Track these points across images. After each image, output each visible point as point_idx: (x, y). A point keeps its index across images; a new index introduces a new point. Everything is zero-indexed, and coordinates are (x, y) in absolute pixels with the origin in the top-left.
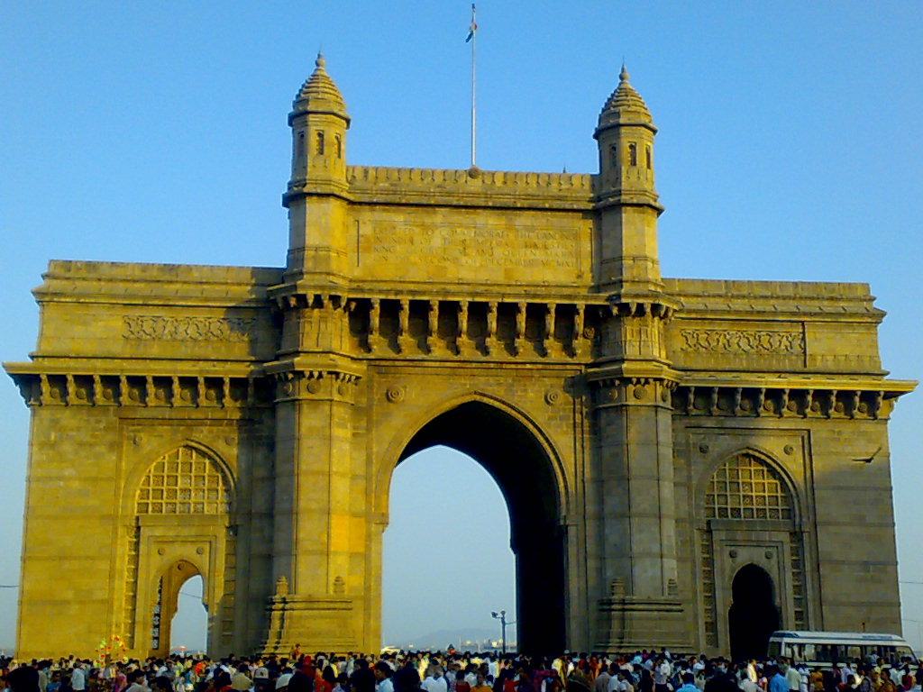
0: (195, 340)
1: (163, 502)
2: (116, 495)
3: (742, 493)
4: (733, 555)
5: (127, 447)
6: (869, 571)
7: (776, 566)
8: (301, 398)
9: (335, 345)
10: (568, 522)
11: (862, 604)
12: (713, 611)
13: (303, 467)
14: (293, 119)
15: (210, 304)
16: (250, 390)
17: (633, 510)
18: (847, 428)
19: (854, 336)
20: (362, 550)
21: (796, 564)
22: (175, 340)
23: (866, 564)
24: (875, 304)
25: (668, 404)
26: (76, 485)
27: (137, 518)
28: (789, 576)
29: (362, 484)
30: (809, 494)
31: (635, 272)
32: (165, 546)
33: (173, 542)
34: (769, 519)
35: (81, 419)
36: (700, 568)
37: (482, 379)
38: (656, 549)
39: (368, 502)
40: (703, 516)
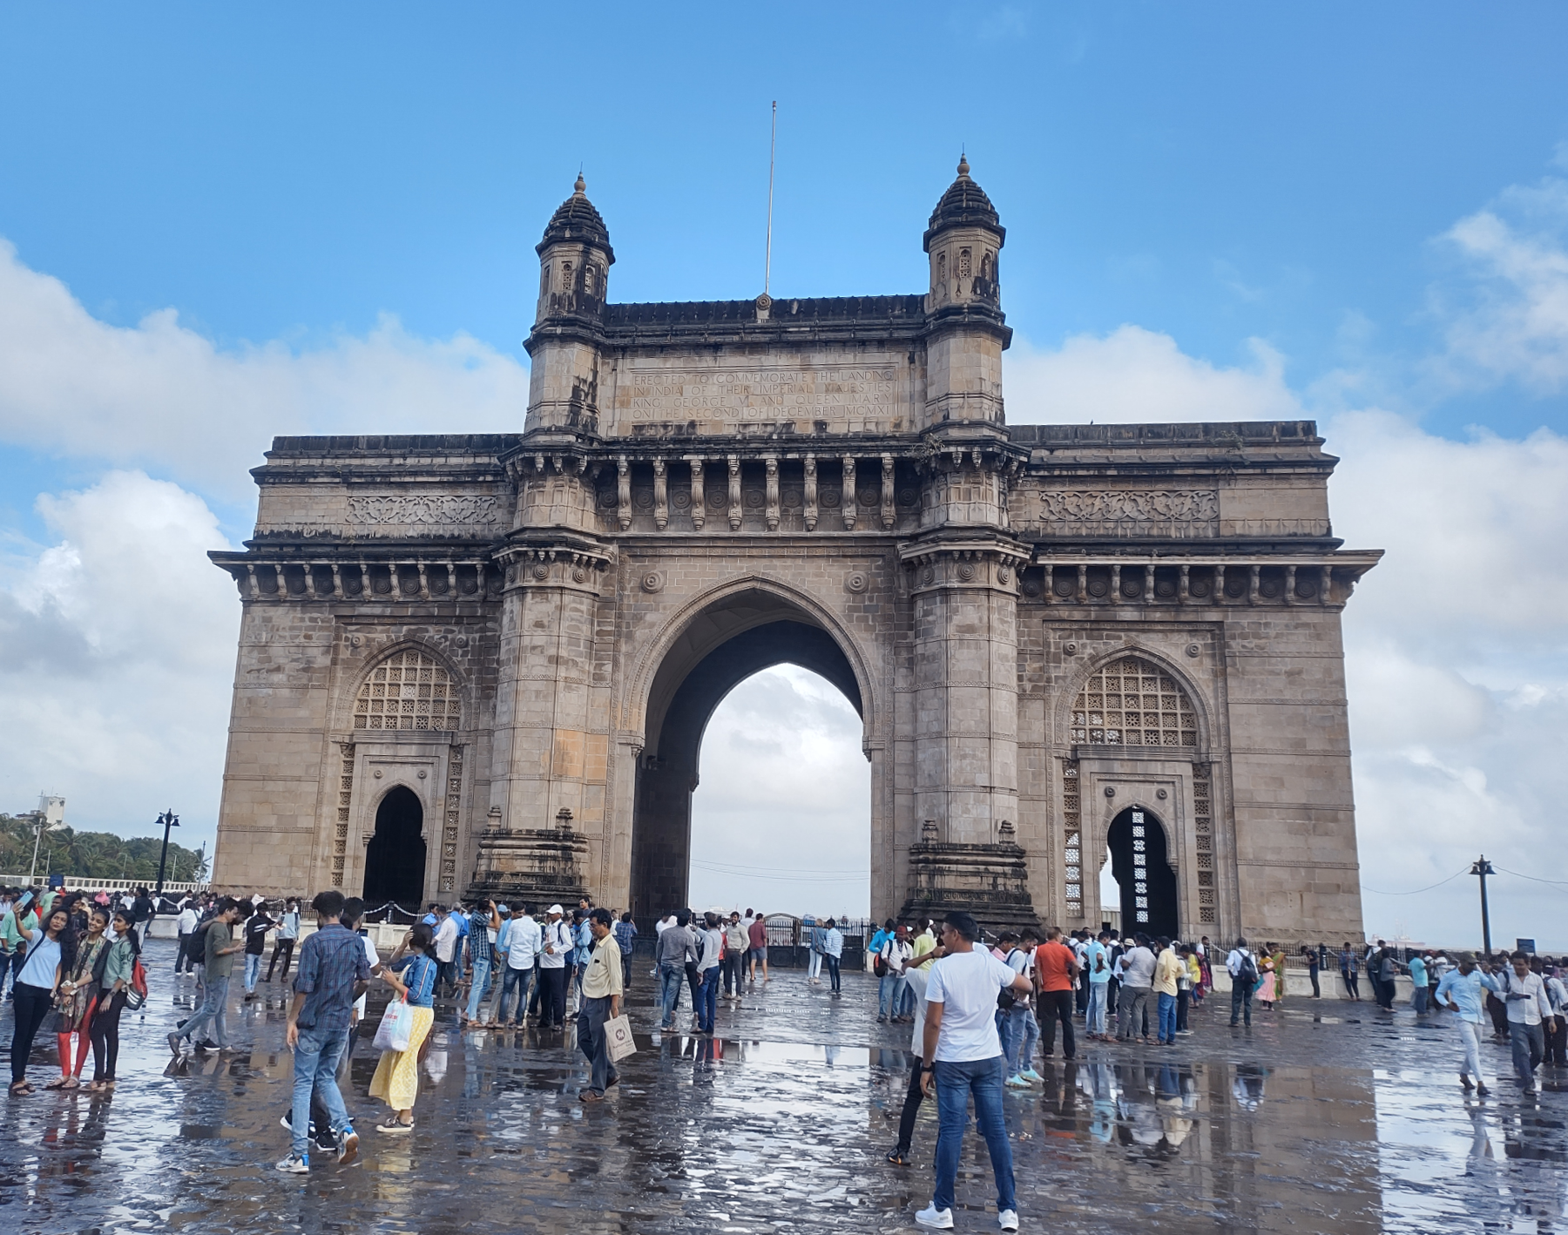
2: (329, 706)
3: (1124, 710)
4: (1109, 794)
5: (345, 654)
6: (1310, 819)
7: (1171, 809)
8: (525, 584)
9: (572, 522)
11: (1294, 866)
14: (541, 250)
15: (445, 479)
16: (480, 580)
17: (953, 728)
18: (1278, 620)
21: (1202, 806)
23: (1305, 809)
24: (1324, 449)
25: (1011, 587)
31: (965, 413)
32: (381, 768)
34: (1162, 744)
37: (765, 562)
38: (982, 780)
40: (1068, 742)
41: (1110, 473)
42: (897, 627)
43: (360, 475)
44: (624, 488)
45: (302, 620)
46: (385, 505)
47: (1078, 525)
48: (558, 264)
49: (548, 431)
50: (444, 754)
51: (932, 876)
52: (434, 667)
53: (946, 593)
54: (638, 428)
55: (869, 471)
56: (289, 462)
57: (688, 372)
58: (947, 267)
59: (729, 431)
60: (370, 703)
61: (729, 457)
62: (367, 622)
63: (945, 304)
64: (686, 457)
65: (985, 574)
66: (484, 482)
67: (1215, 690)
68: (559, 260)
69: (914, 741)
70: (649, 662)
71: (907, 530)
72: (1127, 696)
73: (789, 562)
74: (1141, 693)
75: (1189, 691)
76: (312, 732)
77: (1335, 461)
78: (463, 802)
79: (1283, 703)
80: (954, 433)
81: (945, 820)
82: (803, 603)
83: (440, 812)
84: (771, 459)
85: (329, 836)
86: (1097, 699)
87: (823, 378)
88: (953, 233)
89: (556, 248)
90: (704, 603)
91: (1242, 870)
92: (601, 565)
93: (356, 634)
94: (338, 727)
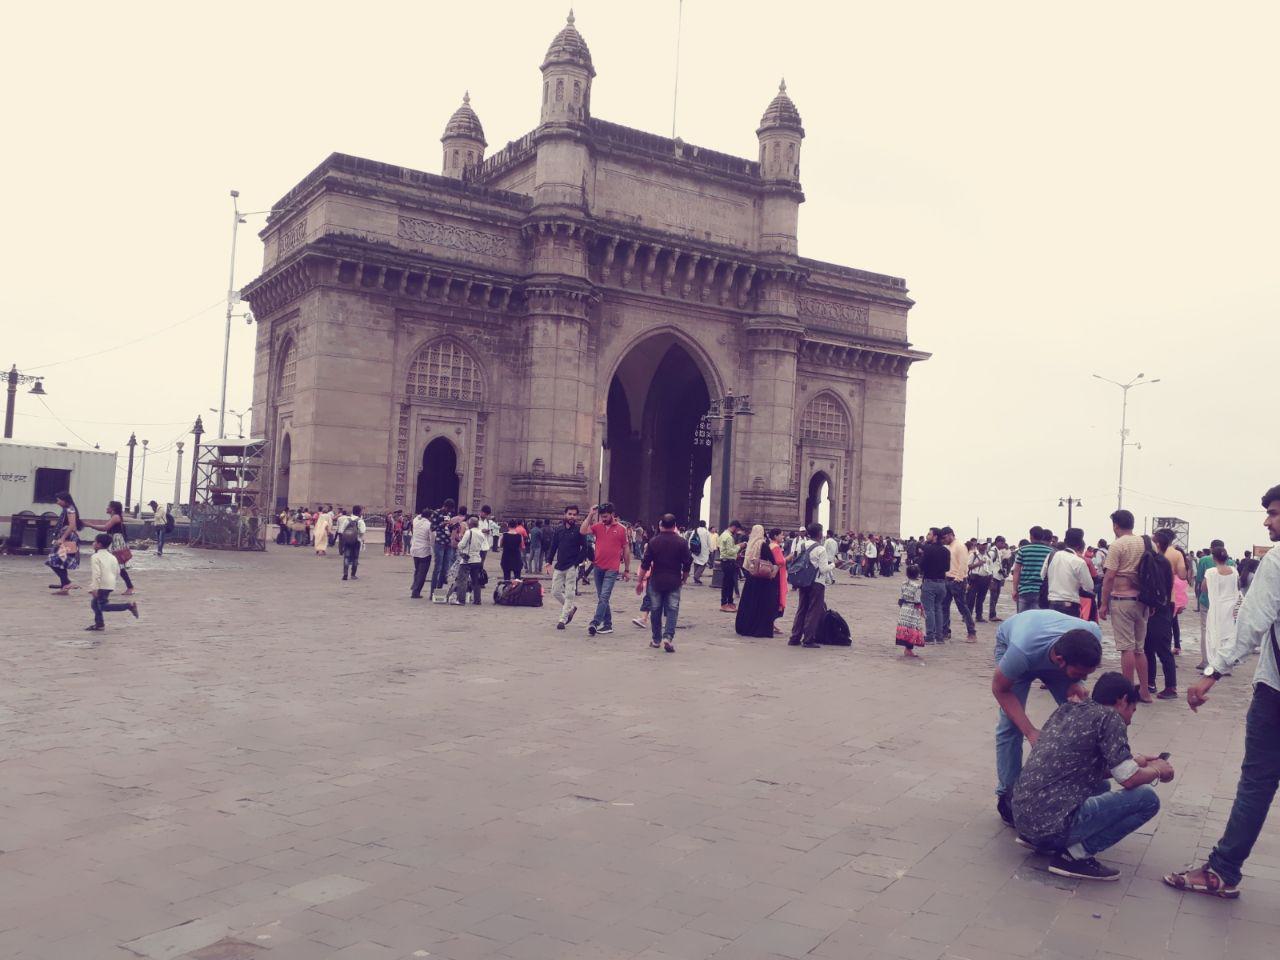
4: (812, 464)
5: (403, 337)
8: (561, 313)
15: (475, 218)
16: (507, 300)
18: (886, 381)
19: (895, 316)
22: (441, 245)
23: (887, 476)
24: (909, 295)
26: (360, 363)
27: (409, 399)
28: (842, 480)
32: (429, 424)
33: (436, 421)
35: (364, 305)
39: (595, 405)
41: (830, 292)
43: (414, 202)
44: (611, 257)
45: (372, 308)
46: (428, 230)
48: (568, 81)
49: (571, 206)
50: (475, 418)
51: (766, 505)
53: (776, 353)
54: (609, 212)
55: (741, 273)
56: (349, 177)
58: (782, 152)
59: (660, 227)
60: (417, 377)
61: (677, 249)
62: (418, 317)
63: (780, 177)
67: (859, 414)
68: (572, 79)
71: (749, 311)
77: (913, 303)
80: (783, 259)
82: (694, 346)
83: (473, 456)
84: (697, 255)
88: (787, 132)
89: (569, 68)
90: (643, 338)
91: (862, 504)
93: (412, 325)
94: (400, 392)
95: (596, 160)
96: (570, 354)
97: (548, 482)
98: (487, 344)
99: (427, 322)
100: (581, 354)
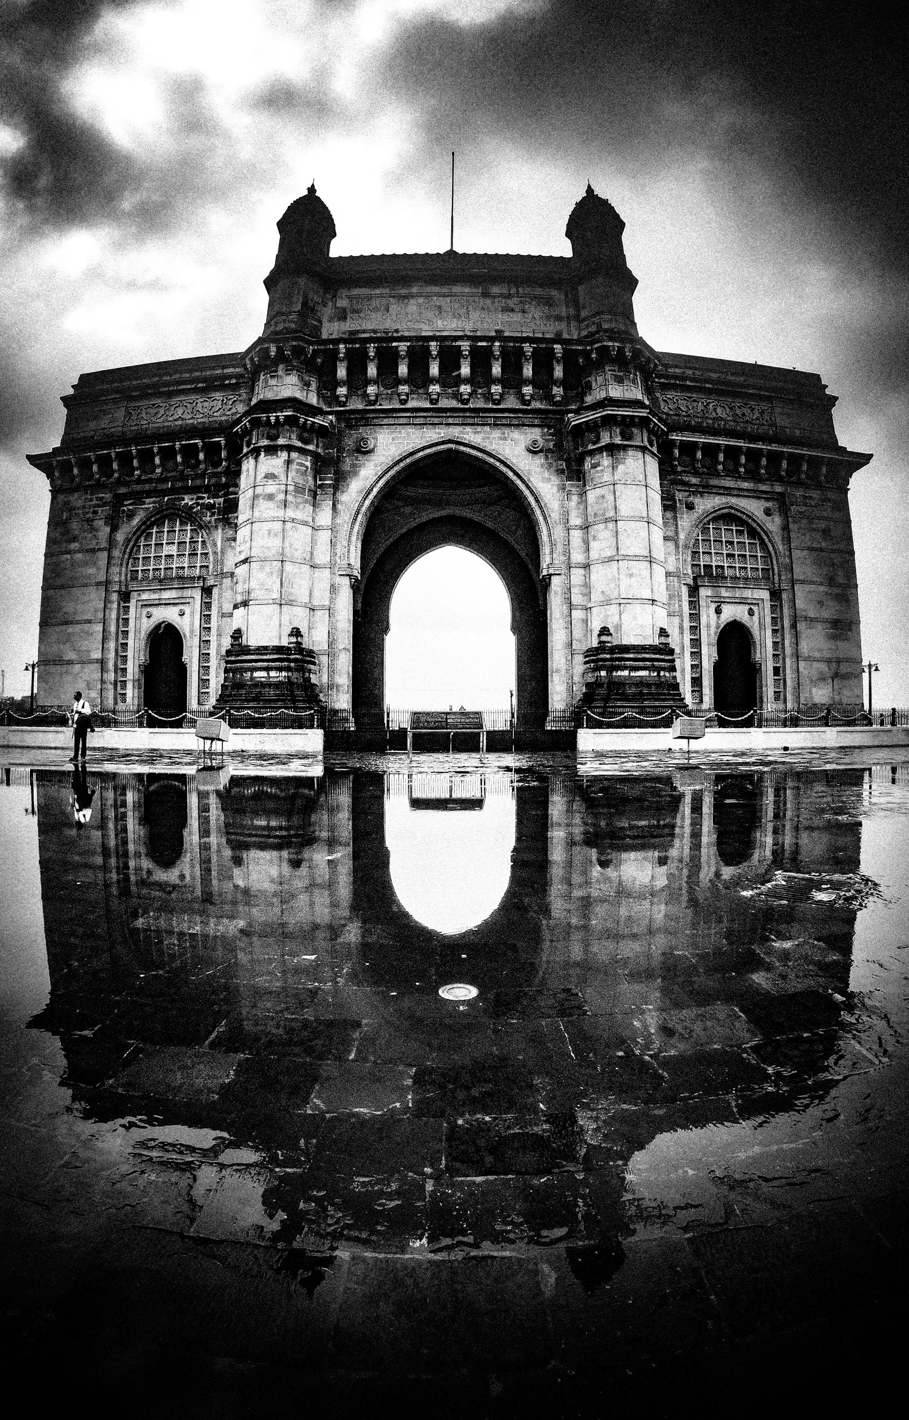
0: (183, 419)
1: (151, 568)
3: (725, 552)
4: (718, 611)
7: (757, 624)
9: (298, 395)
10: (551, 571)
12: (697, 667)
13: (257, 514)
17: (622, 552)
20: (327, 603)
25: (655, 450)
26: (79, 556)
27: (127, 586)
28: (769, 633)
29: (324, 537)
30: (787, 553)
32: (150, 609)
36: (687, 624)
42: (569, 479)
47: (689, 419)
50: (197, 594)
51: (611, 669)
52: (189, 528)
57: (394, 297)
62: (138, 498)
64: (394, 344)
65: (639, 435)
66: (230, 384)
67: (783, 539)
69: (587, 566)
70: (364, 509)
72: (726, 542)
73: (479, 429)
74: (736, 540)
75: (767, 540)
76: (98, 584)
78: (214, 631)
79: (821, 550)
81: (618, 627)
83: (196, 641)
84: (465, 345)
85: (116, 665)
86: (707, 543)
87: (500, 303)
91: (802, 664)
92: (322, 432)
95: (336, 291)
96: (271, 488)
97: (239, 658)
98: (210, 507)
99: (147, 501)
100: (291, 488)
